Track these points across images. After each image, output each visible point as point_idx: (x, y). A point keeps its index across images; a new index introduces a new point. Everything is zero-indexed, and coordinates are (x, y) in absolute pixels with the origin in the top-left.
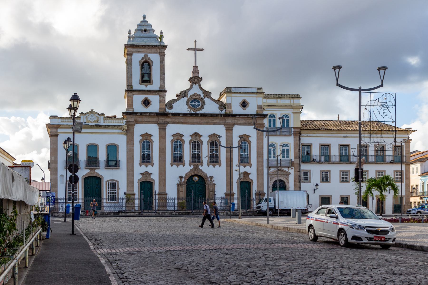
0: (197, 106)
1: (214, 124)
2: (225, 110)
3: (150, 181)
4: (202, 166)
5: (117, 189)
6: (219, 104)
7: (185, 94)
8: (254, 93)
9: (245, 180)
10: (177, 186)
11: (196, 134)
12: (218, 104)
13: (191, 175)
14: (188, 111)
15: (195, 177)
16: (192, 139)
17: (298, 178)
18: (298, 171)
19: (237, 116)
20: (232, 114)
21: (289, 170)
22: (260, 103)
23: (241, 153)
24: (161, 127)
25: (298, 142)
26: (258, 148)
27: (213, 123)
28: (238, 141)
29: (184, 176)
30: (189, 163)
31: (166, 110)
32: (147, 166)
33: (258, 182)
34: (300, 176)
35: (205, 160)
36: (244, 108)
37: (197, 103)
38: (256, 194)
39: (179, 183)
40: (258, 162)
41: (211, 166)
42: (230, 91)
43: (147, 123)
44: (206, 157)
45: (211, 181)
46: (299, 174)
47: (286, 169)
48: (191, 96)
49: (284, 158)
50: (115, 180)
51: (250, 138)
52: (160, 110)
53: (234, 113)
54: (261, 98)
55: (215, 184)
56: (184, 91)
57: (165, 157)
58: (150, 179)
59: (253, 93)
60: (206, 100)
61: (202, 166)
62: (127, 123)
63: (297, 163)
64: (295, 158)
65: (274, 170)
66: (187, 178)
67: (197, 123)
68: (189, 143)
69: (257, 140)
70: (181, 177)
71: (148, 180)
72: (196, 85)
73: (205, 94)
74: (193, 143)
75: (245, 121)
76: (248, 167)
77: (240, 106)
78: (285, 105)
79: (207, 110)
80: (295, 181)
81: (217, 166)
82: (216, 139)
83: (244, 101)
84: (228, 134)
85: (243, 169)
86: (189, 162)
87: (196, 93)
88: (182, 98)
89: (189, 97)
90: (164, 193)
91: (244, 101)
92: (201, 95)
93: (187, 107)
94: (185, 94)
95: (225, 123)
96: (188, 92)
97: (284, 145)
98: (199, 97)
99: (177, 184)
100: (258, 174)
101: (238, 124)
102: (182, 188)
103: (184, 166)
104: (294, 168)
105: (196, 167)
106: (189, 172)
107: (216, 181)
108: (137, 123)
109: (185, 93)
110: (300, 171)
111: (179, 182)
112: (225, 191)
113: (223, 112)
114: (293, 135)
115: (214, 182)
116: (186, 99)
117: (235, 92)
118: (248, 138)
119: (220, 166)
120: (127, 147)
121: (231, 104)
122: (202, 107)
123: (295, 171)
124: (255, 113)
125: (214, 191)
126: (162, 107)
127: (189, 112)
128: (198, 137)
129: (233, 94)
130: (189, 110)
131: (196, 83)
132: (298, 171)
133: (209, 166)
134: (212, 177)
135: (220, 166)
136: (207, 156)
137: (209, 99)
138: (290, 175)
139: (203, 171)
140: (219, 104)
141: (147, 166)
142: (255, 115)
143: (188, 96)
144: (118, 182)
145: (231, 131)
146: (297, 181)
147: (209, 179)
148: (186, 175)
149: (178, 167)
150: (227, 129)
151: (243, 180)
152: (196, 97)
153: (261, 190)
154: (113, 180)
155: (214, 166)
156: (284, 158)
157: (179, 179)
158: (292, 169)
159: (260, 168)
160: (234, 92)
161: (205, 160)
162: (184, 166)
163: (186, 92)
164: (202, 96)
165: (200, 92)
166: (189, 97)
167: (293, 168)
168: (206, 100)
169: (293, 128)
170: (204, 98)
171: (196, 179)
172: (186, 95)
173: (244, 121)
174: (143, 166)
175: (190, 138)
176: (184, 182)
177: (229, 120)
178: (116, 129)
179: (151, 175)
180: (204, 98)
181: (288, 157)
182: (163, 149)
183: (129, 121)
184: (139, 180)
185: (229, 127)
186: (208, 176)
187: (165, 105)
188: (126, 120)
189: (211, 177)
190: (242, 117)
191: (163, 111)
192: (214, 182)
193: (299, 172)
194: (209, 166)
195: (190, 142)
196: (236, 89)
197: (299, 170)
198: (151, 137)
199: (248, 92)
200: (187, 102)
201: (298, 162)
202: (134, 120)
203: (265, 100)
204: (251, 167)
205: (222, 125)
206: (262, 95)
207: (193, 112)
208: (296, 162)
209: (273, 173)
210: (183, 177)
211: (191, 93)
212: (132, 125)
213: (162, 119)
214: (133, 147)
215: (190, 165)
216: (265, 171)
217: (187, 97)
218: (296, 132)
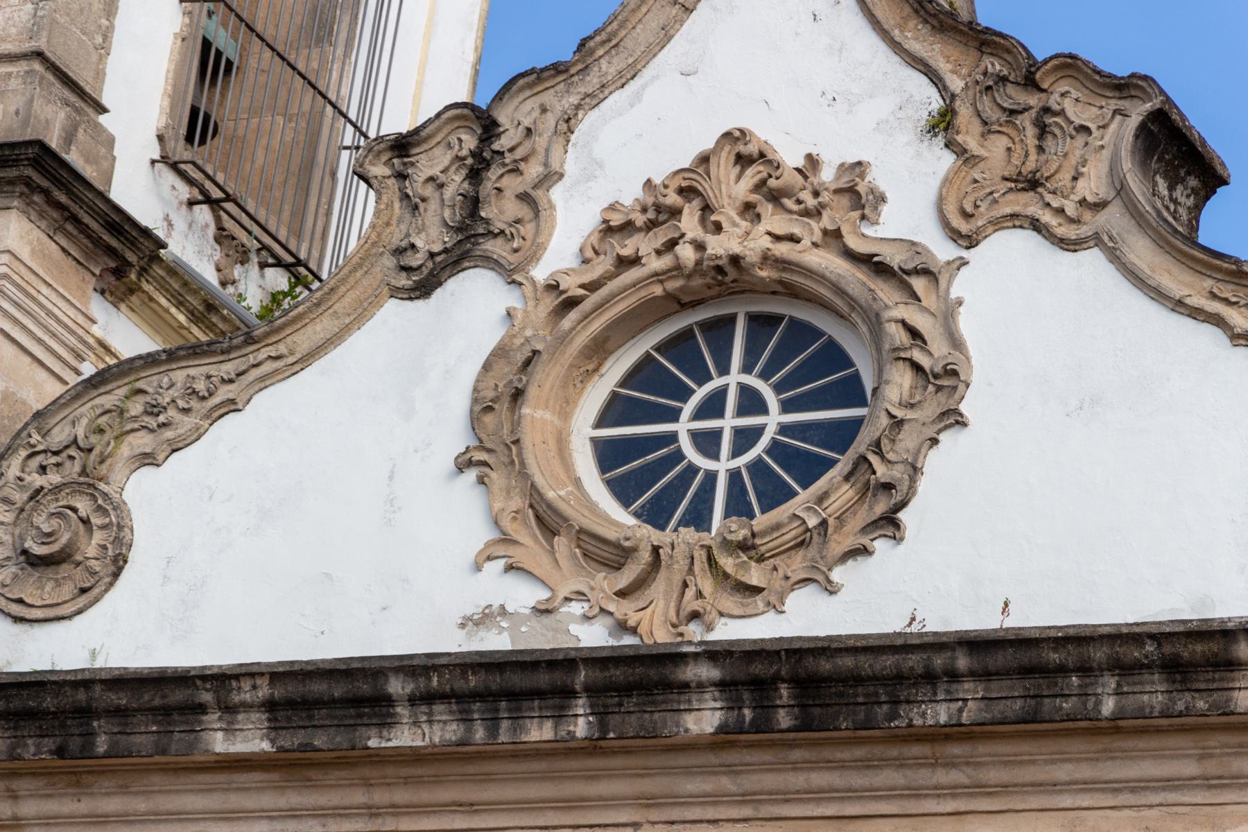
7: (473, 204)
14: (484, 618)
88: (394, 312)
92: (878, 177)
94: (473, 204)
96: (568, 123)
98: (833, 236)
130: (522, 595)
137: (1093, 258)
143: (535, 255)
152: (719, 246)
172: (500, 211)
180: (943, 250)
217: (511, 275)
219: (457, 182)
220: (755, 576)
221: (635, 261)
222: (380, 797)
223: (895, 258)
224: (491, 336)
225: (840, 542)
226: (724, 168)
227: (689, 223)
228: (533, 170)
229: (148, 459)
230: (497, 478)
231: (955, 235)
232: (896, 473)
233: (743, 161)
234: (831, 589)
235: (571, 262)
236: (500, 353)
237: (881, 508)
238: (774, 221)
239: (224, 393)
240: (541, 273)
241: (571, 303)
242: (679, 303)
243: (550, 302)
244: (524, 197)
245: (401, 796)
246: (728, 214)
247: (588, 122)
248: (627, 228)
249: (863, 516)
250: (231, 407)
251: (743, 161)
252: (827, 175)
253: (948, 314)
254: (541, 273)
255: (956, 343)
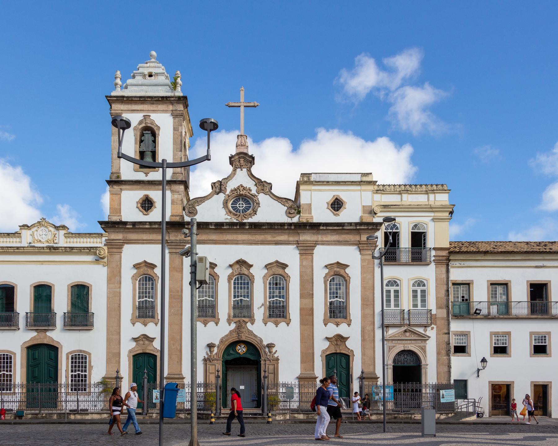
0: (245, 210)
1: (277, 243)
2: (298, 216)
3: (152, 352)
4: (252, 324)
5: (87, 369)
6: (287, 205)
7: (221, 188)
8: (355, 182)
9: (338, 351)
10: (203, 362)
11: (241, 263)
12: (285, 206)
13: (231, 340)
14: (226, 219)
15: (240, 346)
16: (233, 273)
17: (444, 346)
18: (446, 334)
19: (321, 228)
20: (311, 223)
21: (425, 331)
22: (368, 203)
23: (330, 299)
24: (174, 251)
25: (444, 276)
26: (364, 288)
27: (274, 241)
28: (324, 275)
29: (217, 343)
30: (228, 319)
31: (183, 218)
32: (145, 325)
33: (363, 354)
34: (449, 344)
35: (259, 312)
36: (337, 212)
37: (244, 205)
38: (361, 378)
39: (206, 357)
40: (364, 316)
41: (270, 325)
42: (309, 179)
43: (147, 243)
44: (261, 307)
45: (270, 352)
46: (446, 340)
47: (421, 330)
48: (232, 191)
49: (417, 307)
50: (84, 352)
51: (347, 270)
52: (172, 217)
53: (316, 220)
54: (370, 193)
55: (277, 359)
56: (219, 181)
57: (181, 307)
58: (152, 350)
59: (353, 182)
60: (262, 198)
61: (252, 324)
62: (108, 244)
63: (443, 318)
64: (439, 307)
65: (396, 332)
66: (223, 347)
67: (244, 243)
68: (227, 281)
69: (362, 273)
70: (210, 346)
71: (148, 351)
72: (242, 170)
73: (260, 187)
74: (235, 280)
75: (337, 238)
76: (344, 326)
77: (328, 208)
78: (418, 205)
79: (260, 217)
80: (438, 353)
81: (283, 325)
82: (280, 271)
83: (337, 199)
84: (304, 263)
85: (332, 330)
86: (226, 317)
87: (242, 186)
89: (228, 192)
90: (177, 376)
91: (337, 199)
92: (251, 188)
93: (223, 211)
94: (221, 188)
95: (297, 241)
96: (227, 182)
97: (416, 282)
98: (249, 193)
99: (203, 358)
100: (363, 340)
101: (323, 243)
102: (214, 366)
103: (217, 324)
104: (437, 327)
105: (240, 327)
106: (227, 335)
107: (280, 351)
108: (128, 243)
109: (221, 185)
110: (449, 334)
111: (207, 354)
112: (298, 373)
113: (295, 220)
114: (433, 265)
115: (276, 355)
116: (222, 196)
117: (319, 182)
118: (345, 269)
119: (288, 324)
120: (108, 288)
121: (311, 204)
122: (255, 212)
123: (437, 334)
124: (357, 220)
125: (275, 373)
126: (177, 212)
127: (228, 221)
128: (246, 268)
129: (314, 185)
130: (229, 217)
131: (241, 167)
132: (446, 334)
133: (266, 324)
134: (273, 344)
135: (288, 324)
136: (263, 305)
138: (427, 342)
139: (256, 333)
140: (286, 205)
141: (145, 325)
142: (356, 224)
144: (90, 354)
145: (310, 257)
146: (444, 352)
147: (267, 350)
148: (222, 341)
149: (205, 326)
150: (302, 252)
151: (334, 352)
152: (241, 193)
153: (371, 369)
154: (81, 351)
155: (277, 324)
156: (417, 307)
157: (208, 350)
158: (432, 329)
159: (369, 328)
160: (316, 182)
161: (259, 312)
162: (217, 324)
163: (222, 183)
164: (254, 191)
165: (250, 184)
166: (228, 192)
167: (435, 327)
168: (262, 198)
169: (434, 249)
170: (257, 194)
171: (241, 350)
172: (223, 189)
173: (335, 237)
174: (138, 325)
175: (230, 271)
176: (216, 354)
177: (307, 237)
178: (88, 254)
179: (153, 341)
180: (257, 194)
181: (424, 305)
182: (178, 291)
183: (113, 240)
184: (130, 351)
185: (306, 248)
186: (265, 343)
187: (181, 208)
188: (107, 238)
189: (270, 346)
190: (331, 228)
191: (177, 219)
192: (276, 355)
193: (447, 336)
194: (266, 324)
195: (230, 278)
196: (320, 176)
197: (446, 331)
198: (154, 268)
199: (343, 182)
200: (225, 203)
201: (445, 316)
202: (123, 237)
203: (377, 197)
204: (349, 325)
205: (293, 244)
206: (371, 187)
207: (235, 221)
208: (441, 316)
209: (394, 336)
210: (214, 344)
211: (231, 186)
212: (118, 247)
213: (176, 234)
214: (120, 287)
215: (229, 322)
216: (378, 334)
217: (224, 194)
218: (441, 258)
219: (219, 186)
220: (246, 217)
221: (234, 193)
222: (222, 231)
223: (253, 195)
224: (224, 198)
225: (252, 215)
226: (240, 187)
227: (238, 191)
228: (225, 186)
229: (198, 206)
230: (226, 209)
231: (258, 193)
232: (256, 210)
233: (242, 187)
234: (252, 218)
235: (229, 193)
236: (224, 199)
237: (255, 213)
238: (244, 191)
239: (203, 201)
240: (227, 193)
241: (229, 196)
242: (237, 196)
243: (228, 196)
244: (225, 188)
245: (223, 231)
246: (241, 190)
247: (229, 182)
248: (233, 191)
249: (254, 213)
250: (204, 202)
251: (242, 187)
252: (247, 188)
253: (258, 199)
254: (227, 193)
255: (259, 201)
